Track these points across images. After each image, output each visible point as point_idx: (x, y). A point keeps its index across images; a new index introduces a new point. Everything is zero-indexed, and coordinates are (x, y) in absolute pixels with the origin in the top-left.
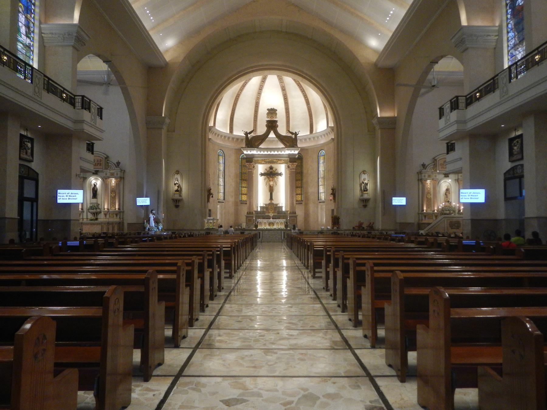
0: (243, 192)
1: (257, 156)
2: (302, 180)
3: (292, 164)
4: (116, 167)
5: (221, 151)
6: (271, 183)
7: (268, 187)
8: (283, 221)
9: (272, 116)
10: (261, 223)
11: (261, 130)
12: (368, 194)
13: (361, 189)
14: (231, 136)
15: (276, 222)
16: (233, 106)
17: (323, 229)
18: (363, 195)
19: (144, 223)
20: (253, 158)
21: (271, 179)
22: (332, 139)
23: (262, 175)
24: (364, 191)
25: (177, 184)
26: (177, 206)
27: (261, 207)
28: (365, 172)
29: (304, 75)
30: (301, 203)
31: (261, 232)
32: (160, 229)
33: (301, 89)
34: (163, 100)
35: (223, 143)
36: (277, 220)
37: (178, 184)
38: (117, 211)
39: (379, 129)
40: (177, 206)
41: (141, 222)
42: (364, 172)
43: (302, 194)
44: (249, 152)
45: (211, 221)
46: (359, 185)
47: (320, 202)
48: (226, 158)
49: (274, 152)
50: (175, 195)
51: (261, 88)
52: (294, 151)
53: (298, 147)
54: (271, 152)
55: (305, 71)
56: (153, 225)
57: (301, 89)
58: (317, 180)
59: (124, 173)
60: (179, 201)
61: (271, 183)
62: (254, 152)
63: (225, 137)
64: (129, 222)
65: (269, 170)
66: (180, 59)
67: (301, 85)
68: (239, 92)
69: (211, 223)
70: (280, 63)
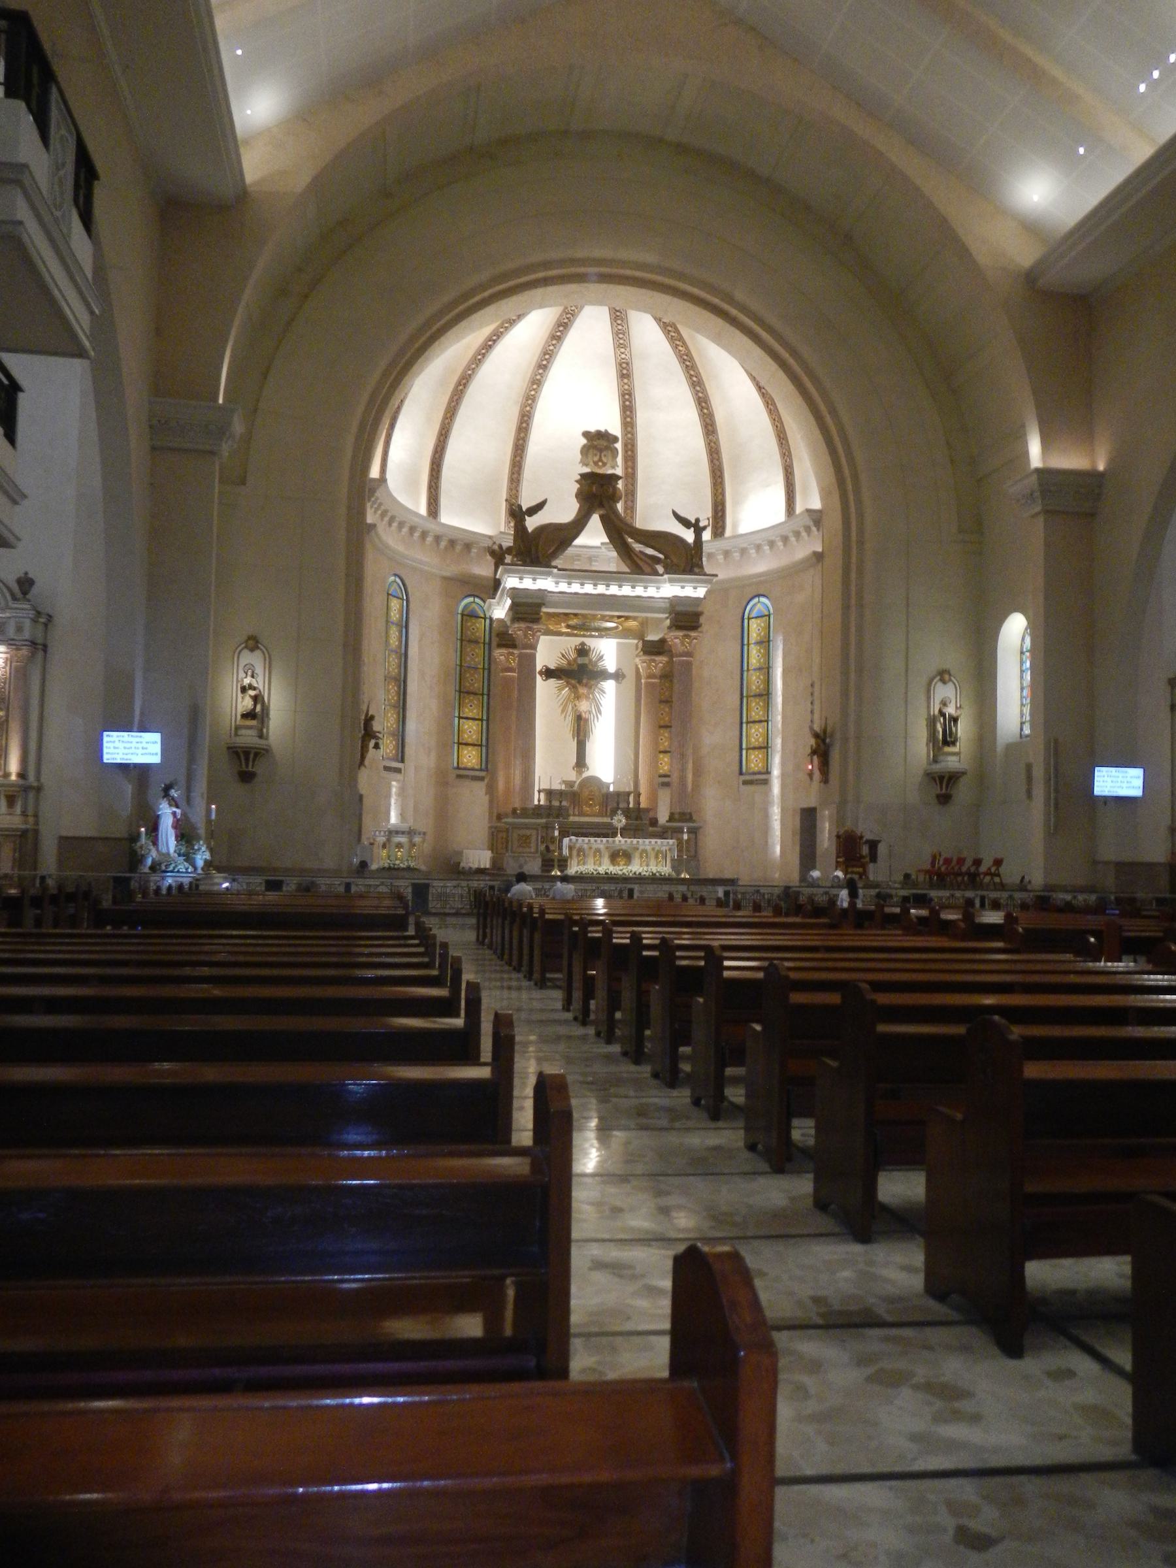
0: (466, 737)
1: (555, 598)
3: (687, 636)
4: (14, 598)
5: (398, 580)
6: (583, 706)
7: (570, 718)
8: (667, 844)
10: (580, 850)
11: (564, 510)
12: (957, 754)
14: (431, 526)
15: (641, 848)
16: (445, 418)
17: (818, 879)
18: (941, 758)
19: (135, 838)
20: (540, 605)
21: (582, 690)
22: (815, 554)
23: (549, 673)
24: (946, 743)
25: (251, 687)
26: (246, 777)
27: (550, 793)
28: (946, 677)
29: (734, 312)
31: (636, 888)
32: (200, 863)
34: (227, 341)
35: (406, 552)
36: (647, 844)
37: (255, 689)
38: (12, 785)
39: (1034, 516)
40: (246, 777)
41: (120, 831)
42: (943, 675)
45: (403, 839)
46: (925, 723)
47: (745, 783)
48: (411, 606)
49: (620, 586)
50: (243, 732)
51: (544, 362)
52: (695, 588)
53: (705, 575)
54: (608, 586)
55: (739, 296)
56: (172, 850)
58: (739, 703)
59: (46, 625)
60: (256, 755)
61: (583, 706)
62: (546, 583)
63: (412, 529)
64: (64, 833)
65: (575, 660)
66: (302, 181)
67: (691, 359)
68: (468, 367)
69: (399, 846)
70: (650, 258)
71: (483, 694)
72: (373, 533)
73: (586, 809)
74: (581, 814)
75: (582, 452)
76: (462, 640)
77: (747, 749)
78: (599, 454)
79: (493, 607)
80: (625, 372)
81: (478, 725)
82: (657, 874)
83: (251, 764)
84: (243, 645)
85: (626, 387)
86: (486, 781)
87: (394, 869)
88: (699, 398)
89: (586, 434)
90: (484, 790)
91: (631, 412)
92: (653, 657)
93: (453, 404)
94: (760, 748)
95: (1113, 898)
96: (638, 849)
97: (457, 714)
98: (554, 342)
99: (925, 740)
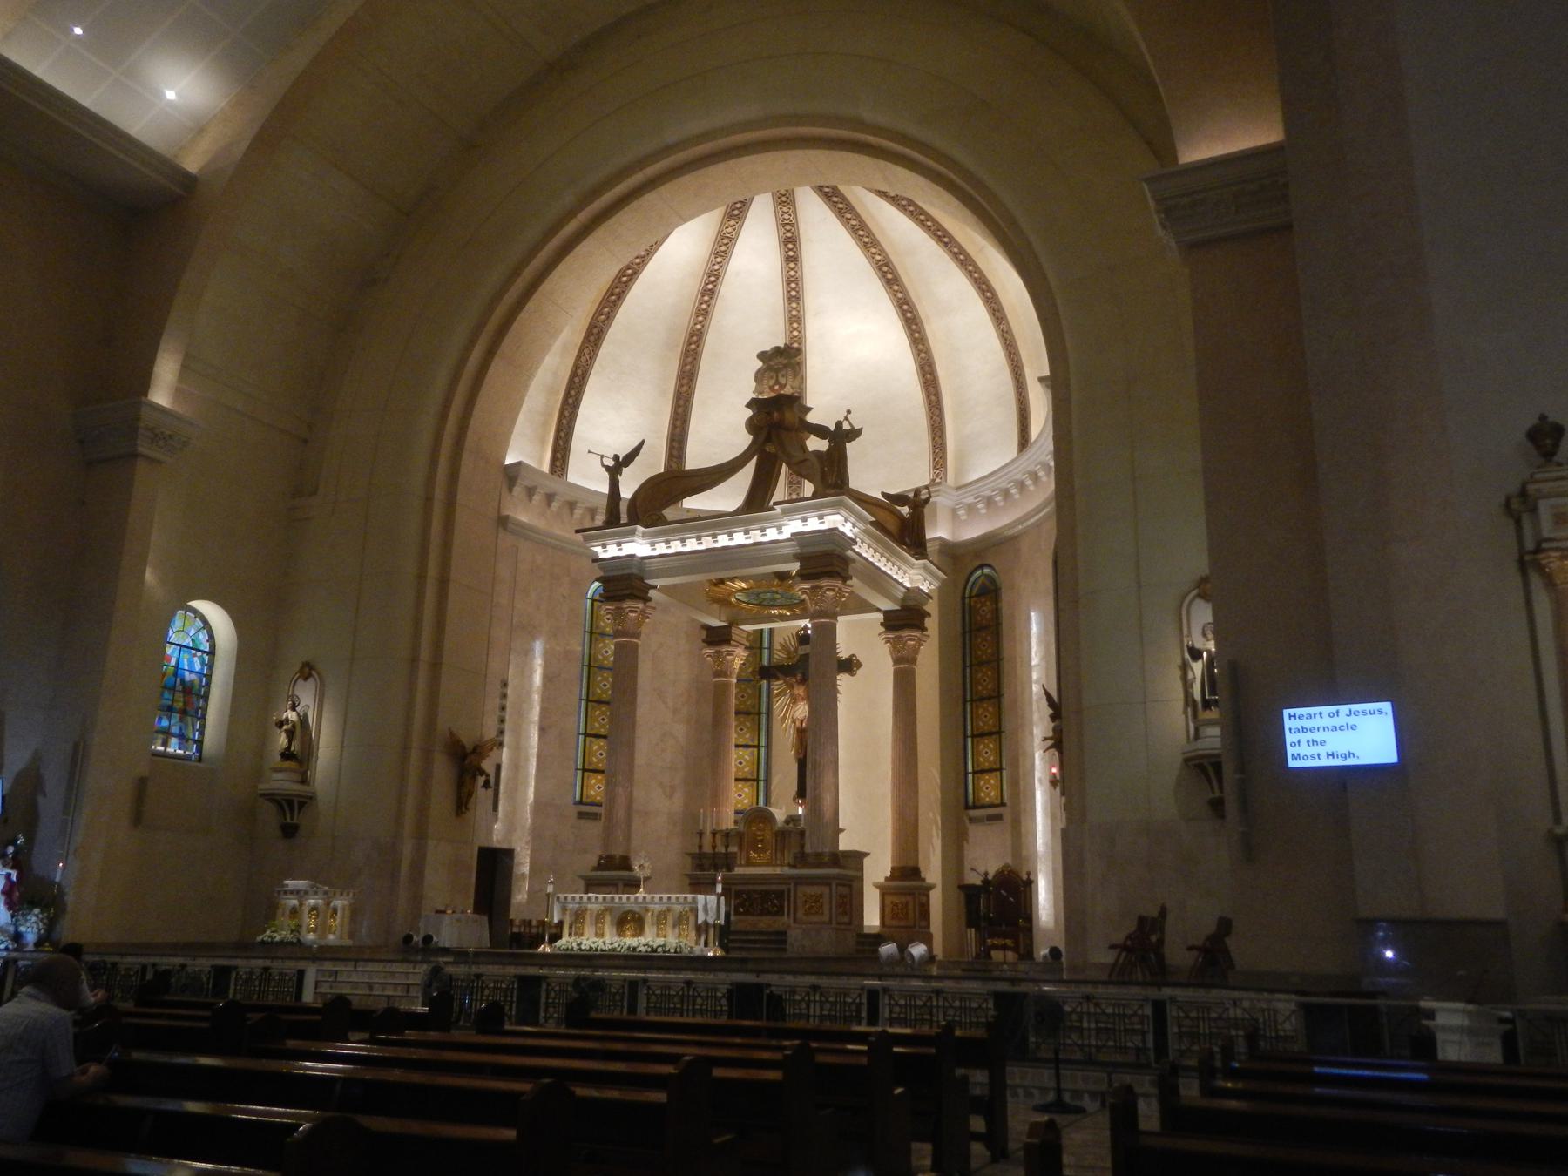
2: (996, 696)
9: (777, 382)
13: (1189, 700)
16: (679, 386)
26: (289, 831)
29: (871, 139)
30: (999, 817)
33: (955, 254)
40: (289, 831)
43: (1000, 770)
44: (612, 551)
49: (730, 534)
52: (821, 517)
54: (714, 536)
55: (868, 115)
57: (955, 254)
62: (638, 547)
65: (796, 650)
72: (510, 525)
73: (753, 854)
74: (749, 863)
75: (756, 379)
78: (774, 375)
80: (889, 276)
81: (752, 753)
82: (660, 950)
83: (296, 817)
84: (298, 675)
85: (900, 295)
88: (975, 279)
89: (762, 356)
93: (688, 367)
95: (1285, 1005)
96: (647, 910)
98: (719, 260)
99: (1180, 704)
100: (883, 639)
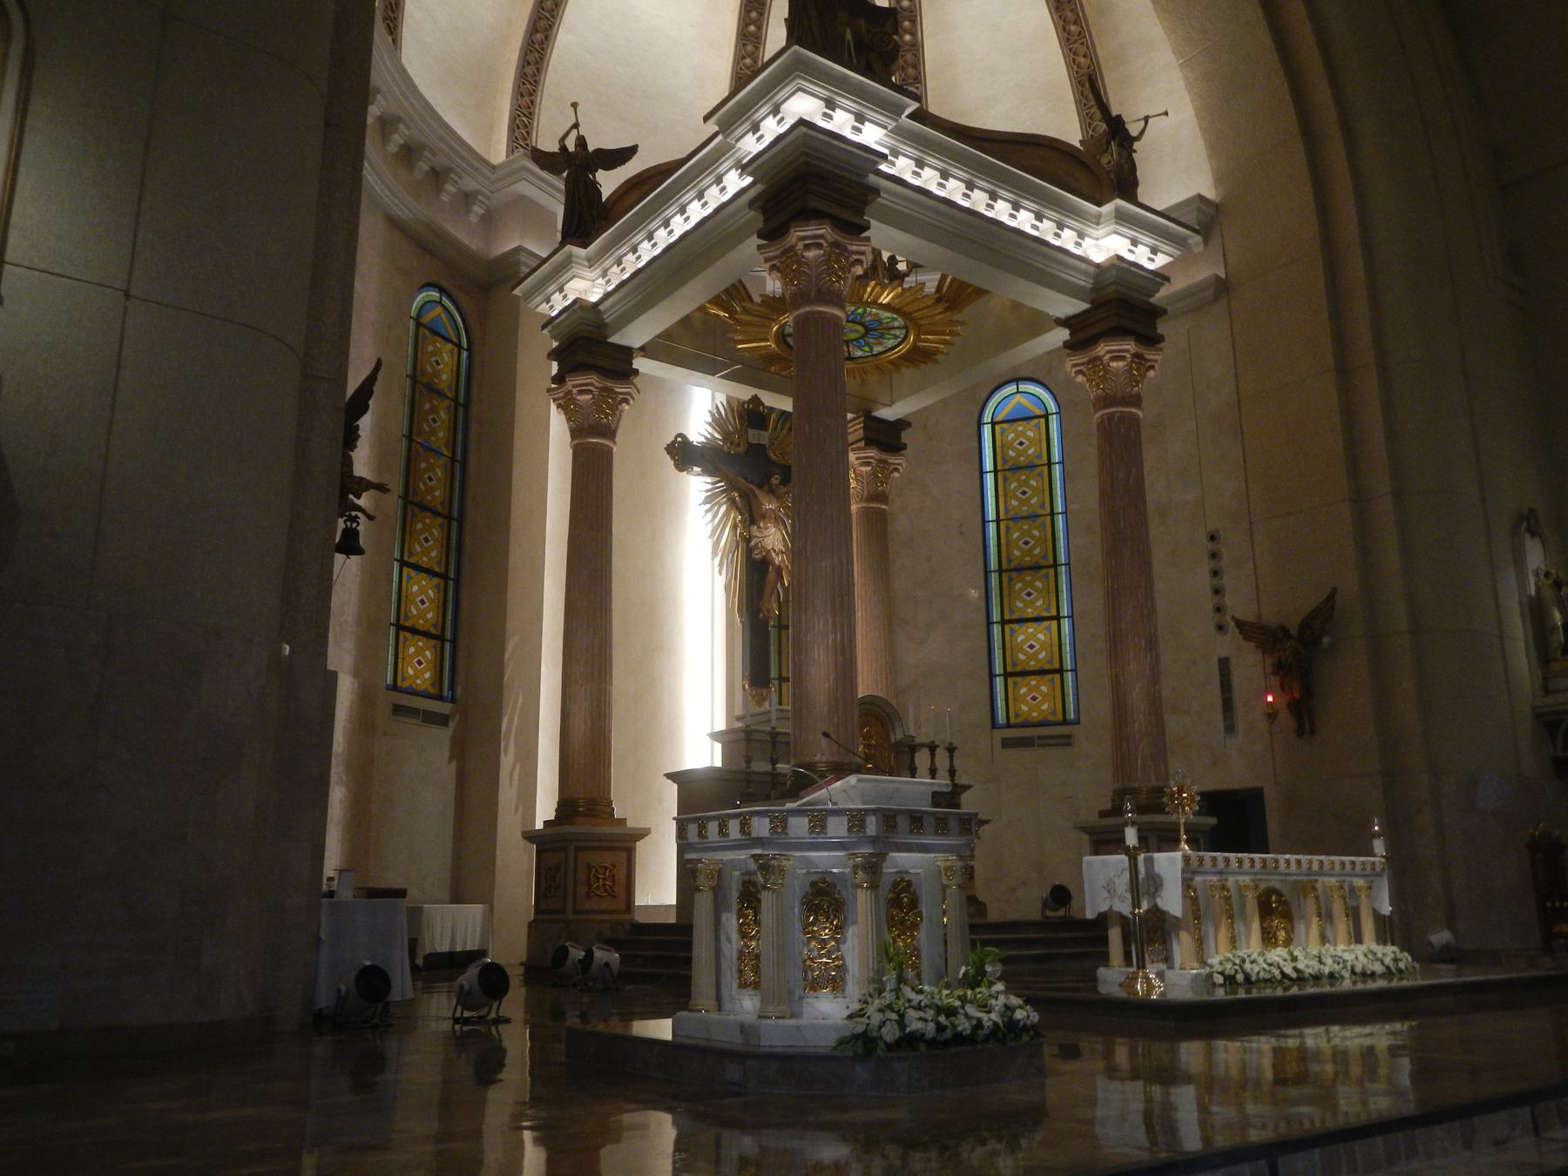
22: (1217, 278)
42: (1528, 523)
44: (841, 122)
47: (1007, 743)
54: (994, 197)
71: (449, 517)
76: (414, 379)
77: (1006, 675)
79: (575, 270)
81: (437, 586)
86: (452, 725)
87: (959, 1039)
90: (447, 744)
91: (761, 14)
92: (883, 457)
94: (1041, 672)
97: (397, 555)
100: (858, 459)
